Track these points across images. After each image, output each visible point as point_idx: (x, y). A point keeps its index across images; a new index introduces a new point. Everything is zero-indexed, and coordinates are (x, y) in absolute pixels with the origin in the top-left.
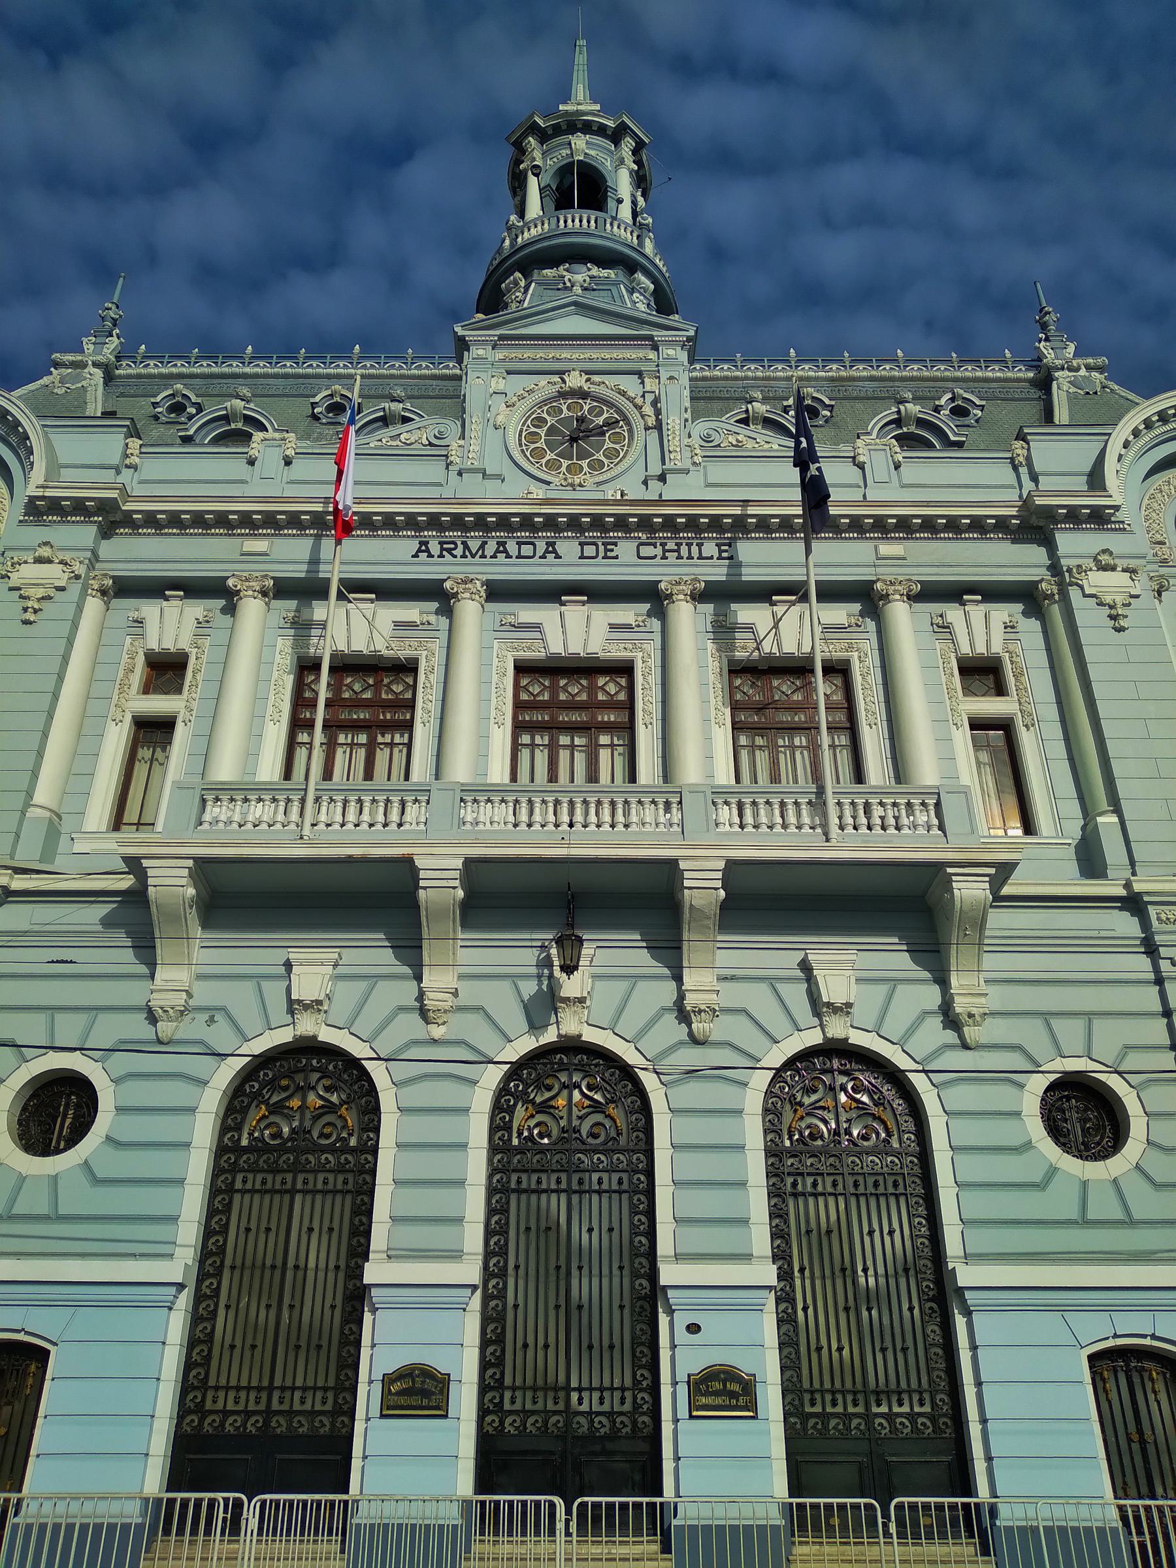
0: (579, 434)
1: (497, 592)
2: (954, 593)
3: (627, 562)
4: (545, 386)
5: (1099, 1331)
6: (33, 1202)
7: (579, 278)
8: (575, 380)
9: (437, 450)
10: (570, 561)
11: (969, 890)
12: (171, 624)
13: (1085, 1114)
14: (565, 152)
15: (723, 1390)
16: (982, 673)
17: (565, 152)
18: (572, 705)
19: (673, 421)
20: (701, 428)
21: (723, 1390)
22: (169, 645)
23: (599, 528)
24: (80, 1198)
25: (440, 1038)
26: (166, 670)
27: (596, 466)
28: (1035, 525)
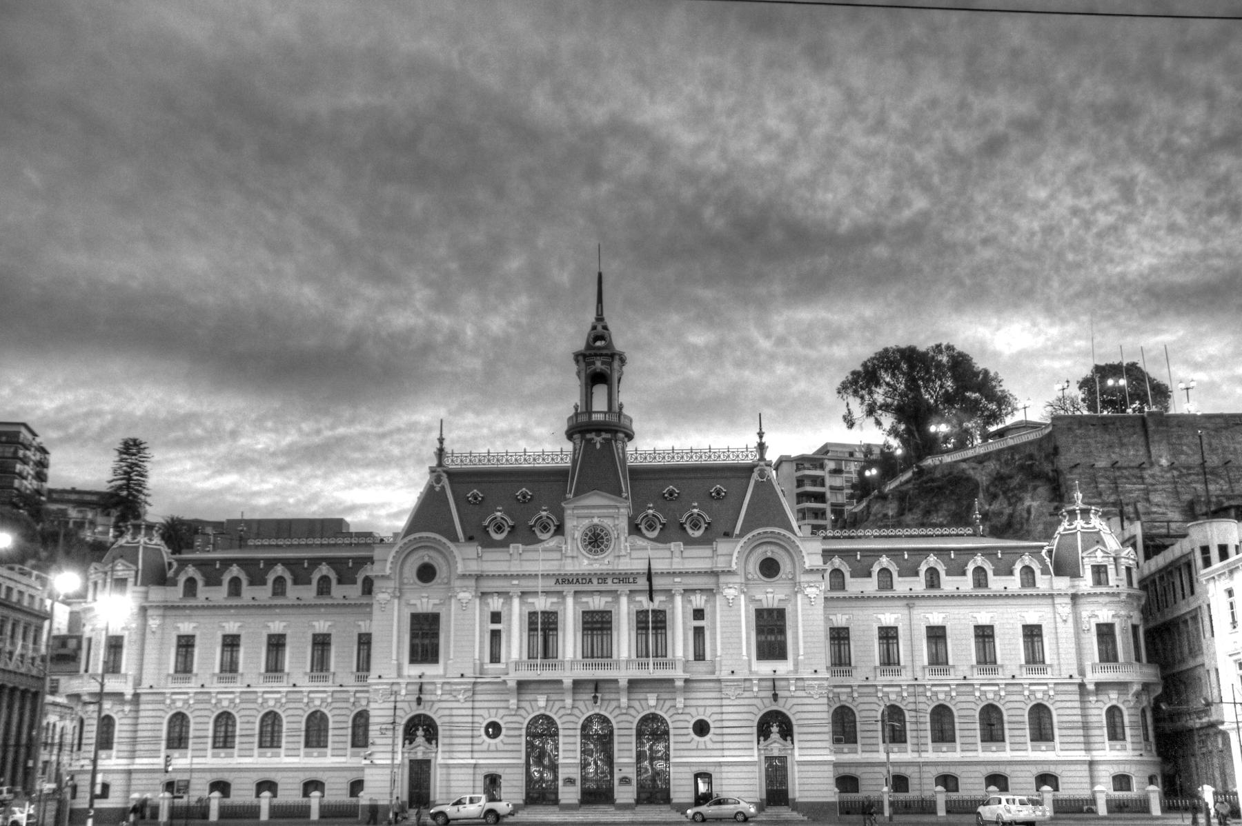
0: (596, 540)
1: (576, 592)
2: (693, 591)
3: (610, 586)
4: (586, 522)
5: (696, 770)
6: (493, 748)
7: (599, 439)
8: (596, 521)
9: (559, 549)
10: (595, 586)
11: (679, 684)
12: (496, 604)
13: (701, 728)
14: (593, 367)
15: (625, 781)
16: (699, 614)
17: (593, 367)
18: (597, 625)
19: (623, 539)
20: (630, 539)
21: (625, 781)
22: (496, 610)
23: (603, 578)
24: (501, 747)
25: (570, 717)
26: (496, 617)
27: (602, 550)
28: (715, 574)
